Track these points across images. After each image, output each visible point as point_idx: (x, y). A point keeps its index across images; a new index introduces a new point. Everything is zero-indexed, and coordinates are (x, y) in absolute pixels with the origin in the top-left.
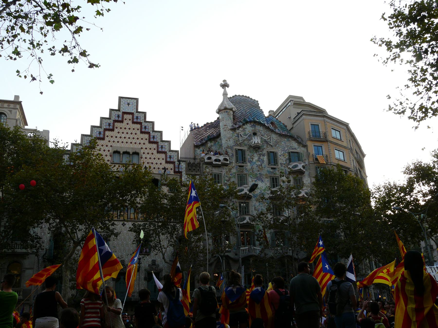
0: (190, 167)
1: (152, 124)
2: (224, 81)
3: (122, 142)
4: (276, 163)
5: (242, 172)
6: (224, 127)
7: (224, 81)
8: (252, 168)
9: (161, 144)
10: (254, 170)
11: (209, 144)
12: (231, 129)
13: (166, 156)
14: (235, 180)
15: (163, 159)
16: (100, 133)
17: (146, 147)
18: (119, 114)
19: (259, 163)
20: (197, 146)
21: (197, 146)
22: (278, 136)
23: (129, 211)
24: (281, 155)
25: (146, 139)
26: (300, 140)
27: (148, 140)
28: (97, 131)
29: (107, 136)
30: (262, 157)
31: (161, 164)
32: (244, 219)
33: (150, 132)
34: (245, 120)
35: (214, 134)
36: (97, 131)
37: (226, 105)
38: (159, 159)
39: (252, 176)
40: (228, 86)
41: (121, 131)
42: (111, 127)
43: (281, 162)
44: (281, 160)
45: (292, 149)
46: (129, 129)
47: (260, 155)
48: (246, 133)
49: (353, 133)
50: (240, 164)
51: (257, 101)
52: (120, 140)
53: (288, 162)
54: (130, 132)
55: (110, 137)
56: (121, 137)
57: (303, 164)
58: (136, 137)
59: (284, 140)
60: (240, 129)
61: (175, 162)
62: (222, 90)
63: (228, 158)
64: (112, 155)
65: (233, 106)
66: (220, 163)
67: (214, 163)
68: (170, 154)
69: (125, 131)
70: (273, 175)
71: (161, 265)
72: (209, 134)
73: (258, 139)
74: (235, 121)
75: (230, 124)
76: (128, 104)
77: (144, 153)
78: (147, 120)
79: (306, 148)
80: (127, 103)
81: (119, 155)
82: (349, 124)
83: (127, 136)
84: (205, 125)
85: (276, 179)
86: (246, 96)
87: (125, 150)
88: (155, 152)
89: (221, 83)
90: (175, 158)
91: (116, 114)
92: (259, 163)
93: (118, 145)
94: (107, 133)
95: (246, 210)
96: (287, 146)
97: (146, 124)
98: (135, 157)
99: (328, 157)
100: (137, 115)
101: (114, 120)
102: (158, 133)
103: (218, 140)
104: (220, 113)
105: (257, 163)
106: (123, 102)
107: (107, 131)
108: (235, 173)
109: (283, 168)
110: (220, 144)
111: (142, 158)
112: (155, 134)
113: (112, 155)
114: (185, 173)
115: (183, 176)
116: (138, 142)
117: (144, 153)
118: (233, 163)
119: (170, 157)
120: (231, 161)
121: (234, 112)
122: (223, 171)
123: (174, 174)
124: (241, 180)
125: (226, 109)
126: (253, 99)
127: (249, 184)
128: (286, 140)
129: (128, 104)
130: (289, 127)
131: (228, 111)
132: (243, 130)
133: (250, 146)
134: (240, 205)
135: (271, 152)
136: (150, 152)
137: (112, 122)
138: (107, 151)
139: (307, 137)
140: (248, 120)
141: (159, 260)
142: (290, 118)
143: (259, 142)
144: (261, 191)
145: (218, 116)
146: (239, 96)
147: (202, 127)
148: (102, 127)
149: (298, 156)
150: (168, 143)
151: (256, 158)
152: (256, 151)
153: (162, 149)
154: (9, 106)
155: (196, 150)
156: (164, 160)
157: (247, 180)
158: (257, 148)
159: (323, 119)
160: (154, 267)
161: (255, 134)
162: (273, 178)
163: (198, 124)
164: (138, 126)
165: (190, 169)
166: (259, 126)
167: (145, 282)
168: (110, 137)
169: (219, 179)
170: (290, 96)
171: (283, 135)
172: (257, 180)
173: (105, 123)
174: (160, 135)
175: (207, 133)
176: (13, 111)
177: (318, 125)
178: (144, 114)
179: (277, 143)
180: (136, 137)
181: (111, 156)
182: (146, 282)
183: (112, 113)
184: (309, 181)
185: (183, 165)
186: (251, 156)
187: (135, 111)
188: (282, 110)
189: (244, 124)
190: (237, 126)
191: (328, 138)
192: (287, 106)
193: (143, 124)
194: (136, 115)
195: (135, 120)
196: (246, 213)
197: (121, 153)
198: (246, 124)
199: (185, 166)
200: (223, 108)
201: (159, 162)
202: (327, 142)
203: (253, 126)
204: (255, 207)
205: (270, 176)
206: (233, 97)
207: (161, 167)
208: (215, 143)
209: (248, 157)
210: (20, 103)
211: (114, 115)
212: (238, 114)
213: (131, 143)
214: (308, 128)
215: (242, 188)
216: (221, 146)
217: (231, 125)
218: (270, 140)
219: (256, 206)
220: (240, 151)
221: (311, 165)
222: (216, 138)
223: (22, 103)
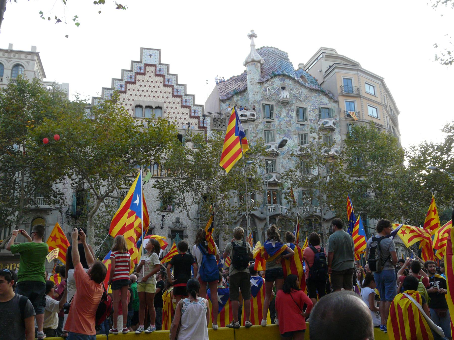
0: (215, 123)
1: (175, 76)
2: (252, 31)
3: (145, 96)
4: (305, 118)
5: (270, 128)
6: (251, 81)
8: (280, 124)
9: (185, 98)
10: (282, 126)
11: (235, 98)
12: (258, 83)
13: (190, 111)
14: (261, 136)
15: (187, 114)
16: (121, 86)
17: (170, 101)
18: (141, 66)
19: (288, 119)
20: (222, 101)
21: (222, 101)
22: (308, 90)
23: (152, 167)
25: (170, 93)
26: (331, 95)
27: (171, 94)
28: (118, 84)
29: (129, 90)
30: (290, 113)
31: (185, 119)
32: (271, 177)
34: (273, 73)
35: (241, 88)
36: (118, 84)
37: (253, 56)
38: (183, 113)
39: (279, 132)
40: (255, 36)
41: (143, 84)
42: (133, 80)
43: (310, 118)
44: (310, 116)
46: (152, 82)
47: (289, 110)
48: (275, 87)
49: (388, 89)
50: (268, 120)
51: (287, 53)
52: (143, 94)
53: (318, 118)
54: (152, 85)
55: (131, 90)
56: (143, 91)
57: (333, 121)
58: (159, 90)
59: (315, 95)
60: (268, 83)
61: (199, 117)
62: (249, 41)
63: (255, 113)
64: (134, 109)
65: (261, 58)
66: (246, 119)
68: (194, 109)
69: (148, 84)
70: (301, 132)
71: (185, 223)
72: (235, 88)
73: (287, 93)
74: (263, 74)
75: (257, 77)
76: (151, 55)
78: (170, 72)
79: (337, 103)
80: (149, 55)
81: (141, 109)
82: (383, 78)
83: (150, 89)
84: (231, 78)
85: (305, 135)
86: (275, 48)
87: (147, 105)
88: (179, 106)
89: (249, 34)
90: (199, 112)
91: (137, 66)
92: (288, 119)
93: (141, 99)
94: (129, 86)
95: (273, 168)
96: (317, 102)
97: (169, 77)
98: (159, 111)
99: (361, 113)
100: (160, 67)
101: (135, 73)
102: (182, 86)
103: (245, 94)
104: (247, 65)
105: (285, 119)
106: (145, 53)
107: (129, 84)
109: (312, 124)
110: (247, 98)
111: (165, 112)
112: (179, 87)
113: (134, 109)
114: (210, 128)
116: (161, 95)
117: (167, 107)
118: (260, 118)
119: (195, 112)
121: (262, 65)
122: (250, 127)
123: (198, 129)
124: (268, 137)
125: (253, 61)
126: (282, 50)
127: (277, 140)
128: (316, 95)
129: (151, 55)
130: (320, 82)
131: (256, 63)
133: (279, 101)
134: (267, 162)
135: (300, 107)
136: (174, 106)
137: (134, 74)
138: (128, 105)
139: (339, 91)
140: (277, 74)
141: (183, 217)
142: (321, 71)
143: (288, 97)
144: (289, 148)
145: (245, 68)
146: (268, 47)
147: (228, 80)
148: (124, 80)
149: (329, 112)
150: (192, 97)
151: (284, 114)
152: (285, 106)
153: (186, 103)
154: (26, 57)
155: (222, 104)
156: (189, 115)
157: (274, 137)
158: (285, 103)
159: (355, 72)
160: (178, 224)
161: (283, 88)
162: (302, 135)
163: (223, 78)
164: (161, 79)
165: (215, 125)
166: (288, 80)
167: (168, 240)
168: (131, 90)
170: (322, 47)
171: (313, 89)
172: (285, 136)
173: (126, 76)
174: (184, 88)
175: (233, 86)
176: (31, 62)
177: (351, 79)
178: (167, 66)
179: (306, 98)
180: (159, 90)
181: (133, 110)
182: (170, 239)
183: (134, 65)
184: (340, 139)
187: (158, 62)
188: (312, 63)
189: (272, 78)
190: (265, 80)
191: (361, 93)
192: (318, 59)
193: (166, 77)
194: (159, 67)
195: (158, 73)
196: (272, 171)
197: (144, 107)
198: (275, 78)
199: (210, 121)
200: (250, 60)
201: (183, 117)
202: (360, 97)
206: (261, 48)
207: (185, 122)
208: (241, 98)
209: (276, 112)
210: (37, 54)
211: (136, 67)
212: (266, 67)
213: (154, 96)
214: (340, 83)
215: (269, 144)
216: (248, 100)
217: (258, 78)
218: (300, 95)
219: (283, 164)
220: (268, 106)
221: (342, 122)
222: (242, 92)
223: (39, 54)
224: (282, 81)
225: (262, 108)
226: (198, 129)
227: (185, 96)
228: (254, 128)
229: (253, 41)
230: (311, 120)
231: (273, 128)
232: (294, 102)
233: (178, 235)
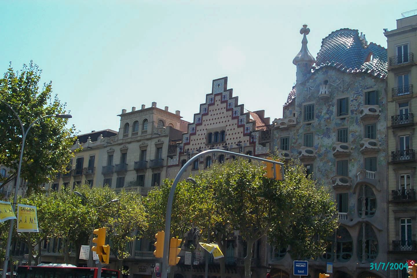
5: (309, 130)
7: (305, 26)
10: (321, 125)
13: (244, 129)
19: (328, 116)
24: (353, 100)
31: (240, 138)
33: (233, 108)
36: (197, 118)
39: (318, 133)
45: (368, 88)
47: (329, 106)
50: (307, 122)
60: (311, 81)
66: (286, 126)
67: (281, 127)
70: (341, 127)
71: (236, 233)
77: (228, 130)
80: (218, 85)
87: (215, 131)
88: (236, 127)
91: (210, 98)
101: (208, 104)
105: (325, 117)
108: (301, 133)
114: (258, 142)
115: (256, 146)
116: (224, 120)
117: (228, 130)
120: (299, 121)
122: (291, 133)
123: (249, 145)
128: (361, 79)
129: (219, 85)
132: (314, 81)
144: (326, 148)
151: (324, 111)
161: (326, 82)
165: (263, 138)
169: (286, 143)
172: (323, 136)
181: (206, 138)
184: (385, 126)
185: (257, 135)
186: (320, 109)
187: (223, 90)
194: (224, 94)
201: (238, 136)
203: (325, 72)
204: (319, 169)
205: (338, 129)
209: (316, 112)
211: (209, 99)
219: (320, 167)
224: (325, 74)
225: (303, 111)
226: (249, 145)
227: (241, 116)
228: (295, 134)
229: (305, 37)
230: (352, 112)
231: (312, 130)
232: (335, 95)
233: (231, 244)
